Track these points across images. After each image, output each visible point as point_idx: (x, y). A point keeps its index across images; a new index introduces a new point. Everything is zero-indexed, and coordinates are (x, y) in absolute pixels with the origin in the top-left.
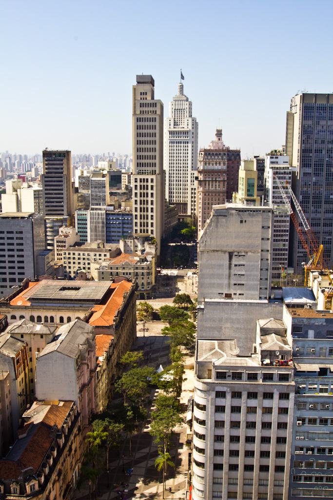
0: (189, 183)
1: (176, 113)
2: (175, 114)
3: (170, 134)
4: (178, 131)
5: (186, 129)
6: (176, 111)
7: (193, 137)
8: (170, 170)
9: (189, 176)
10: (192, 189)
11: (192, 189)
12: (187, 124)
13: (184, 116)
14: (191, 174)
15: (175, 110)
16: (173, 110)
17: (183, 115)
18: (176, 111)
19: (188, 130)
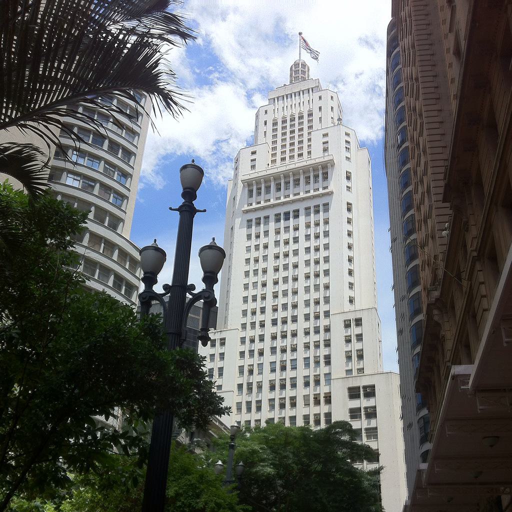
0: (339, 366)
1: (279, 132)
2: (275, 136)
3: (251, 195)
4: (286, 176)
5: (318, 156)
6: (279, 126)
7: (348, 188)
8: (244, 326)
9: (338, 334)
10: (354, 393)
11: (354, 393)
12: (322, 147)
13: (309, 133)
14: (347, 325)
15: (275, 124)
16: (270, 124)
17: (305, 132)
18: (279, 126)
19: (326, 159)
